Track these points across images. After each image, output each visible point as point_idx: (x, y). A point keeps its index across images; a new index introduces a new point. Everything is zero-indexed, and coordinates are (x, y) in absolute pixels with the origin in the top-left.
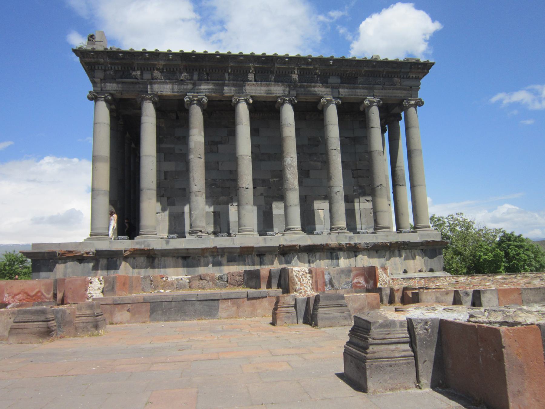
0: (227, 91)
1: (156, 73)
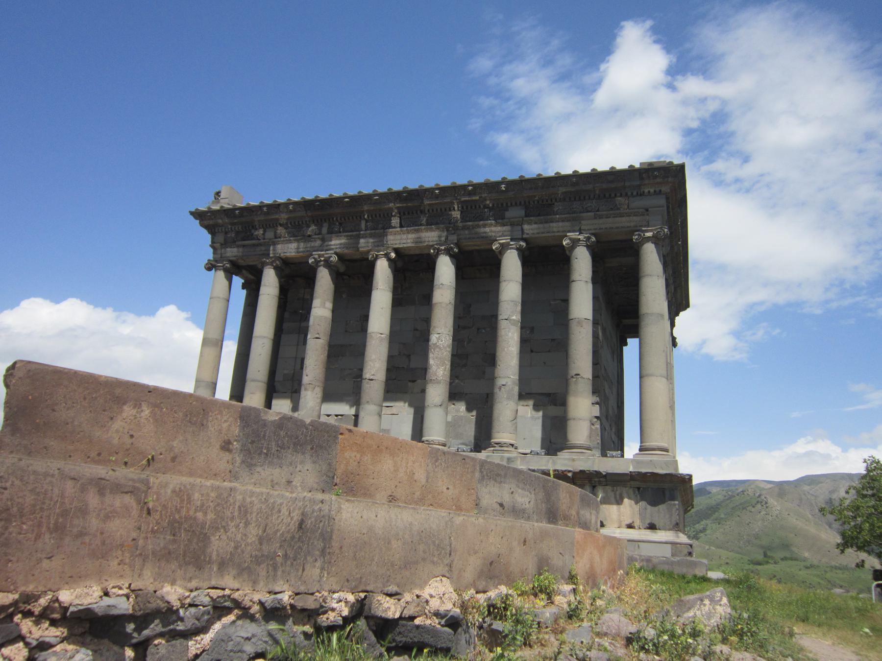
0: (363, 245)
1: (281, 230)
